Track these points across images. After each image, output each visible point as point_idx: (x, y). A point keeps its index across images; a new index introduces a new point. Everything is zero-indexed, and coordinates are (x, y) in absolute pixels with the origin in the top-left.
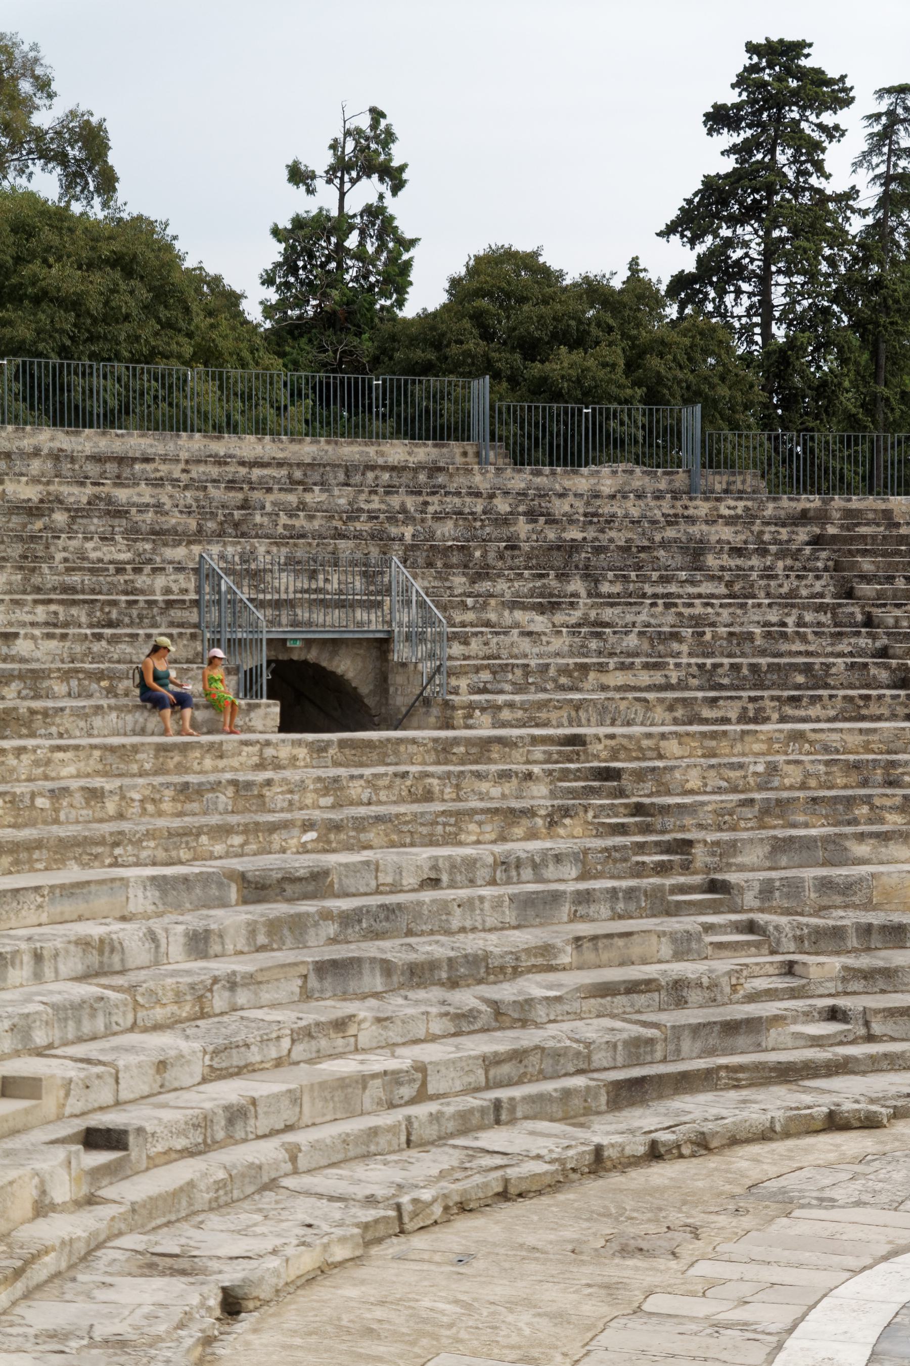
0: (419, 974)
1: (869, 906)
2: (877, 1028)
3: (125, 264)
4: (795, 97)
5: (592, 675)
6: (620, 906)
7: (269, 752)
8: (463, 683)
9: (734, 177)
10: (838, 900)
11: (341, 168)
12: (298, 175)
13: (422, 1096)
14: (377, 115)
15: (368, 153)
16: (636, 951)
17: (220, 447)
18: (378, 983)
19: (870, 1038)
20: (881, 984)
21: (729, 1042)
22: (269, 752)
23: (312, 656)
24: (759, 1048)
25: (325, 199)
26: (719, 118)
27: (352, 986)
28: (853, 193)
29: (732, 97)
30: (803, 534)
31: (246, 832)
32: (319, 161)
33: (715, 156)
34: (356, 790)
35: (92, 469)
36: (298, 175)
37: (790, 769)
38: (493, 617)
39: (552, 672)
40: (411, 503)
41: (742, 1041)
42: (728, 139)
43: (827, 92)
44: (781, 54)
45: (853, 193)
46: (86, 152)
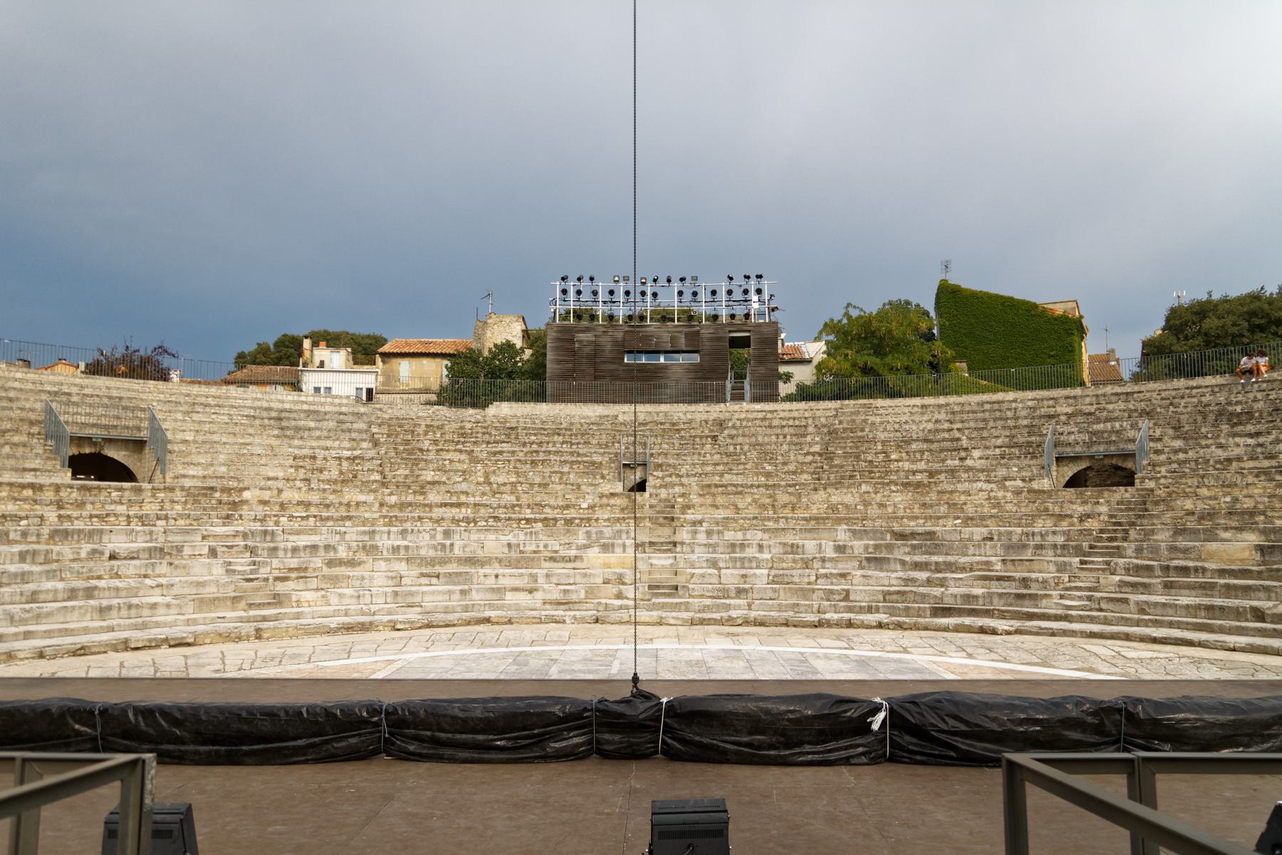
1: (1199, 559)
2: (1103, 606)
3: (1253, 314)
5: (1234, 464)
6: (1059, 552)
7: (992, 494)
8: (1163, 469)
10: (1181, 555)
16: (1036, 566)
17: (1193, 383)
18: (899, 567)
19: (1101, 610)
20: (1141, 589)
21: (1020, 602)
22: (992, 494)
23: (1114, 461)
24: (1036, 606)
27: (885, 567)
31: (925, 518)
35: (1114, 398)
37: (1247, 500)
38: (1223, 441)
39: (1212, 462)
40: (1259, 396)
41: (1026, 602)
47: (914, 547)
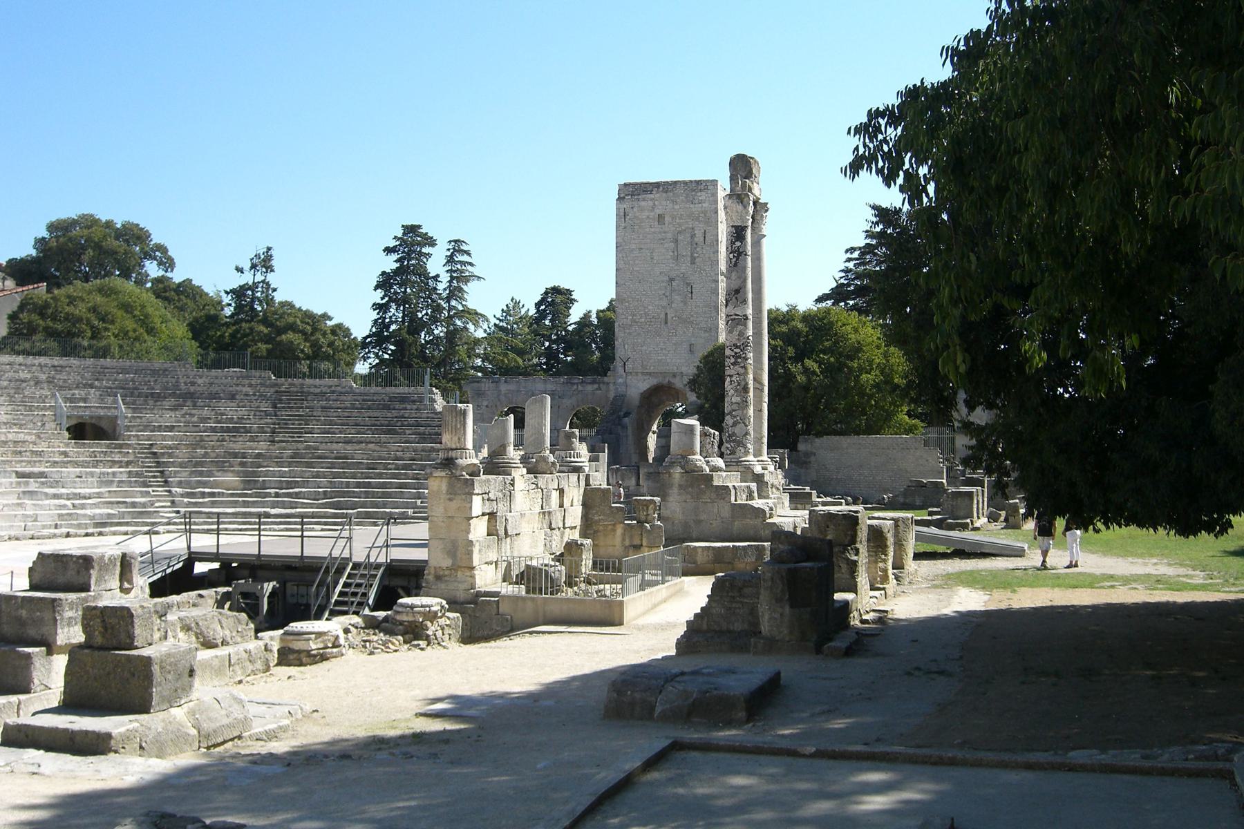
0: (56, 496)
4: (419, 244)
9: (396, 272)
11: (253, 267)
12: (240, 270)
13: (36, 520)
14: (269, 249)
15: (264, 262)
25: (247, 278)
26: (388, 250)
28: (438, 276)
29: (393, 243)
30: (272, 390)
32: (247, 266)
33: (390, 263)
34: (71, 454)
36: (240, 270)
42: (395, 256)
43: (431, 242)
44: (411, 230)
45: (438, 276)
46: (168, 263)
47: (43, 483)
